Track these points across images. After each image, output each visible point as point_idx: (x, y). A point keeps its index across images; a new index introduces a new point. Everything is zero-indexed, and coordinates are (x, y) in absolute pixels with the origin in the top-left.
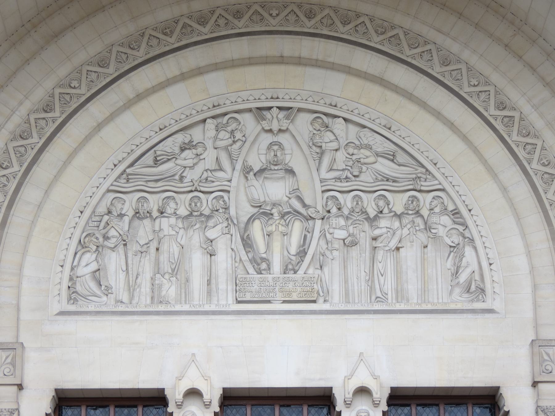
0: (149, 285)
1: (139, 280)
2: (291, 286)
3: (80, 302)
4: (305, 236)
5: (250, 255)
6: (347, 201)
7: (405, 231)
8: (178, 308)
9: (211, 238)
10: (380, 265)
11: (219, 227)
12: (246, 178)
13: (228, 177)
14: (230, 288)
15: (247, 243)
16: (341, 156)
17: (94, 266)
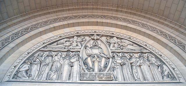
0: (46, 75)
1: (43, 73)
2: (102, 75)
3: (18, 79)
4: (106, 63)
5: (86, 67)
6: (120, 54)
7: (142, 61)
8: (56, 81)
9: (72, 61)
10: (135, 70)
11: (76, 59)
12: (86, 48)
13: (80, 48)
14: (78, 76)
15: (85, 63)
16: (116, 45)
17: (27, 68)
